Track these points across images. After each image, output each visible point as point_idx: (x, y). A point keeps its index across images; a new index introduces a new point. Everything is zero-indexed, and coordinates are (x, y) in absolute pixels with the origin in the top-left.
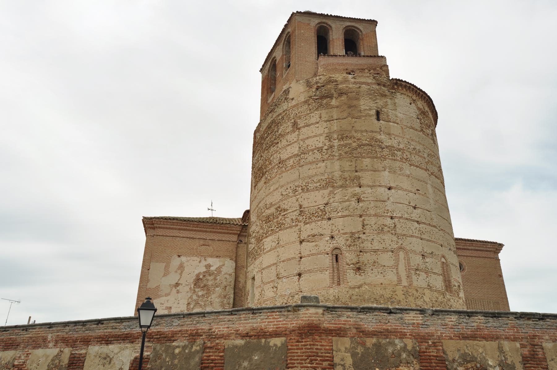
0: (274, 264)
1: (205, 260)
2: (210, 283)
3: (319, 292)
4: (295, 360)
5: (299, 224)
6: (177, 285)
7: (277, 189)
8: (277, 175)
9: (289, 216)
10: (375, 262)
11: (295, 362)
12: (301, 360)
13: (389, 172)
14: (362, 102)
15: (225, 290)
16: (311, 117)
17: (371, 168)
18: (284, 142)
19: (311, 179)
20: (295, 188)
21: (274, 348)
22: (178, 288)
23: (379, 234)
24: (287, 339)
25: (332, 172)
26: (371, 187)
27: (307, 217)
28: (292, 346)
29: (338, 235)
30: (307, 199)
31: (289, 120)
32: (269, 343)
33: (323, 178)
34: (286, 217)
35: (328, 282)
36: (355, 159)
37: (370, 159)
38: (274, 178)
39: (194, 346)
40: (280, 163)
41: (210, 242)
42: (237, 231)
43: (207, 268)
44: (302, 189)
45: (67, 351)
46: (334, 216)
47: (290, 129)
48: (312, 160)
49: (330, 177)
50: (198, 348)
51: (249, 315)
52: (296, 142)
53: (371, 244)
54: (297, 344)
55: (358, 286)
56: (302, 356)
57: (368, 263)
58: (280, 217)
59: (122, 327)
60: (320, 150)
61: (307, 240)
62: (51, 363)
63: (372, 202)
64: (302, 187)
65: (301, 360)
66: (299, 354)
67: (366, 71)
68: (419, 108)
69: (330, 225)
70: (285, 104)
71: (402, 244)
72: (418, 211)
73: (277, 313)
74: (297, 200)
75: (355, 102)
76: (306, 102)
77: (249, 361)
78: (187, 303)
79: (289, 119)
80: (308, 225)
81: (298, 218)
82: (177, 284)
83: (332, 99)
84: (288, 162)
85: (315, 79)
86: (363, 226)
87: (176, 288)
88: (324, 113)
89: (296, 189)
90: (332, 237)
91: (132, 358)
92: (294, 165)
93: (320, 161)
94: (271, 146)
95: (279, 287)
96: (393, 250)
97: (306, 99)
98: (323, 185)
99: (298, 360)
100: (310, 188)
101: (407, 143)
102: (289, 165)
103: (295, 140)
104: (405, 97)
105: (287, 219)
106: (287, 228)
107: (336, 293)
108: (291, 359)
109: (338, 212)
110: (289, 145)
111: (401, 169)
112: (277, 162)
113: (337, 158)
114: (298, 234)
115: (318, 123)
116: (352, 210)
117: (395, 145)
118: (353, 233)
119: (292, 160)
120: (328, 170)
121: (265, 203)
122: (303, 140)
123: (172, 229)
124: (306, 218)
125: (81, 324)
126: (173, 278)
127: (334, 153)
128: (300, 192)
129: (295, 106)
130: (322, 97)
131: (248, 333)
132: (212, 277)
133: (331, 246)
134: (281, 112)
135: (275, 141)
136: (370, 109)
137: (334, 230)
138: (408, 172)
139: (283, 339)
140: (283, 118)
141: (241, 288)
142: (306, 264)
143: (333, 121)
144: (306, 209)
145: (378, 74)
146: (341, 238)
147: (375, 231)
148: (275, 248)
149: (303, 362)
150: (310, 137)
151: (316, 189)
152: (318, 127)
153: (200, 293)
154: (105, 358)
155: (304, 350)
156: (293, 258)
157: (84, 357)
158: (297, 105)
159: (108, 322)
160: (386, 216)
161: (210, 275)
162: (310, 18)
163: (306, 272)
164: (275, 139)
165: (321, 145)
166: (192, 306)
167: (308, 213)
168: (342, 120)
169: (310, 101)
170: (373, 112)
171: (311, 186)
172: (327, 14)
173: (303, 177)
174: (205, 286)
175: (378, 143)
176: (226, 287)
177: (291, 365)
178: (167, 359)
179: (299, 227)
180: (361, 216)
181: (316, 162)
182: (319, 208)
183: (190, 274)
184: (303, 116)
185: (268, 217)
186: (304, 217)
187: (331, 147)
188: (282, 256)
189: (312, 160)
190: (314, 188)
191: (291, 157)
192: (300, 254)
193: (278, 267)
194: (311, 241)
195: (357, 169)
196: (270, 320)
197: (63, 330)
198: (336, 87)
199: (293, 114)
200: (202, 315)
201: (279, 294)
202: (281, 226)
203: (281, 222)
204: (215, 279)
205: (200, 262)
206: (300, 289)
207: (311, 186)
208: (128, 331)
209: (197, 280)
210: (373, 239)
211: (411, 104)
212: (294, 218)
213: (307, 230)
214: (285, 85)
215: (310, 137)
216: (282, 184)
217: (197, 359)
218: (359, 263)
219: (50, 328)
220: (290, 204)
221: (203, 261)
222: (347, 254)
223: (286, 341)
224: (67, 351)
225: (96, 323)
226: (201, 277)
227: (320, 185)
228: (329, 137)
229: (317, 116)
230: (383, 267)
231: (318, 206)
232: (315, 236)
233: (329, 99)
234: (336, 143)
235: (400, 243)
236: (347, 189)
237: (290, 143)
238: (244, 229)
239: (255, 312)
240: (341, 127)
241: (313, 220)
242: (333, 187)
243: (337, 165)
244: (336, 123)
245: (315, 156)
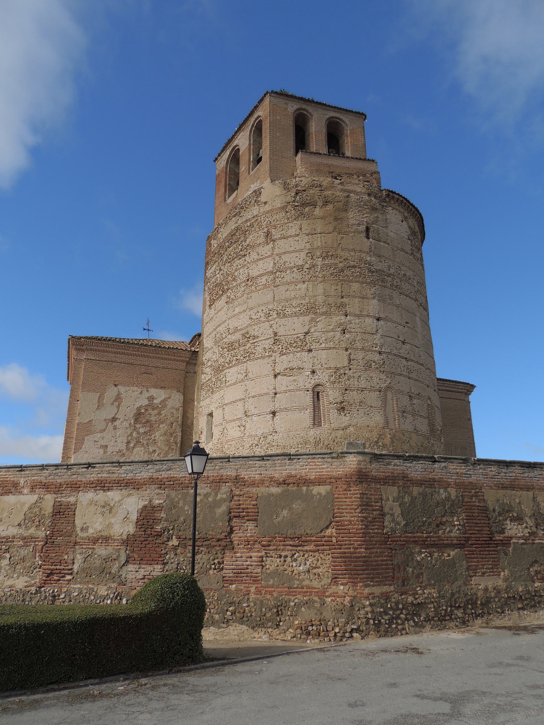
0: (240, 400)
1: (148, 391)
2: (153, 418)
3: (298, 433)
4: (343, 509)
5: (274, 354)
6: (114, 419)
7: (244, 311)
8: (245, 295)
9: (260, 344)
10: (361, 402)
11: (344, 511)
12: (351, 509)
13: (378, 300)
14: (351, 215)
15: (172, 427)
16: (290, 227)
17: (359, 295)
18: (254, 256)
19: (288, 303)
20: (268, 312)
21: (318, 496)
22: (115, 424)
23: (367, 371)
24: (333, 487)
25: (314, 296)
26: (359, 316)
27: (283, 347)
28: (339, 494)
29: (320, 369)
30: (284, 325)
31: (261, 229)
32: (311, 491)
33: (303, 302)
34: (257, 345)
35: (308, 421)
36: (341, 282)
37: (358, 283)
38: (240, 297)
39: (219, 494)
40: (248, 280)
41: (153, 370)
42: (185, 357)
43: (149, 401)
44: (277, 314)
45: (49, 499)
46: (316, 347)
47: (262, 239)
48: (290, 280)
49: (312, 301)
50: (224, 496)
51: (285, 461)
52: (269, 256)
53: (358, 381)
54: (345, 492)
55: (341, 428)
56: (352, 505)
57: (354, 403)
58: (249, 345)
59: (122, 472)
60: (300, 268)
61: (284, 374)
62: (29, 511)
63: (360, 333)
64: (277, 311)
65: (351, 509)
66: (348, 503)
67: (355, 177)
68: (410, 227)
69: (311, 358)
70: (255, 208)
71: (390, 383)
72: (406, 347)
73: (320, 460)
74: (271, 327)
75: (343, 214)
76: (283, 208)
77: (289, 510)
78: (126, 441)
79: (260, 227)
80: (284, 357)
81: (272, 347)
82: (113, 418)
83: (315, 208)
84: (259, 280)
85: (294, 181)
86: (350, 360)
87: (112, 424)
88: (305, 224)
89: (269, 313)
90: (313, 372)
91: (140, 507)
92: (267, 283)
93: (299, 282)
94: (235, 258)
95: (248, 426)
96: (380, 389)
97: (283, 205)
98: (304, 311)
99: (346, 509)
100: (287, 313)
101: (398, 268)
102: (260, 284)
103: (269, 253)
104: (397, 213)
105: (257, 348)
106: (258, 358)
107: (317, 435)
108: (338, 509)
109: (321, 344)
110: (260, 259)
111: (391, 298)
112: (245, 279)
113: (320, 279)
114: (272, 366)
115: (298, 235)
116: (337, 342)
117: (385, 270)
118: (338, 369)
119: (264, 278)
120: (311, 294)
121: (228, 327)
122: (279, 255)
123: (107, 352)
124: (282, 348)
125: (64, 467)
126: (109, 412)
127: (317, 273)
128: (275, 317)
129: (268, 212)
130: (304, 205)
131: (284, 481)
132: (156, 412)
133: (313, 382)
134: (249, 217)
135: (241, 253)
136: (359, 225)
137: (316, 364)
138: (398, 302)
139: (328, 487)
140: (252, 225)
141: (190, 425)
142: (282, 401)
143: (316, 235)
144: (282, 338)
145: (368, 182)
146: (324, 374)
147: (362, 367)
148: (242, 381)
149: (353, 511)
150: (289, 252)
151: (295, 314)
152: (298, 241)
153: (142, 430)
154: (104, 507)
155: (353, 499)
156: (266, 394)
157: (75, 504)
158: (272, 210)
159: (102, 465)
160: (375, 351)
161: (153, 410)
162: (288, 102)
163: (281, 410)
165: (300, 263)
166: (132, 445)
167: (285, 342)
168: (328, 235)
169: (288, 208)
170: (363, 228)
171: (289, 311)
172: (309, 99)
173: (279, 300)
174: (147, 421)
175: (367, 265)
176: (172, 423)
177: (338, 515)
178: (186, 508)
179: (273, 358)
180: (347, 350)
181: (296, 283)
182: (298, 337)
183: (129, 407)
184: (279, 226)
185: (231, 344)
186: (280, 346)
187: (313, 266)
188: (251, 390)
189: (290, 280)
190: (292, 313)
191: (261, 275)
192: (275, 389)
193: (246, 403)
194: (288, 375)
195: (343, 294)
196: (311, 467)
197: (39, 473)
198: (321, 193)
199: (266, 222)
200: (226, 460)
201: (247, 434)
202: (249, 356)
203: (250, 350)
204: (159, 414)
205: (141, 393)
206: (274, 429)
207: (289, 311)
208: (130, 476)
209: (138, 416)
210: (360, 376)
211: (402, 221)
212: (266, 347)
213: (283, 362)
214: (253, 184)
215: (289, 252)
216: (250, 306)
217: (223, 508)
218: (343, 402)
219: (21, 471)
220: (261, 330)
221: (145, 392)
222: (331, 392)
223: (331, 490)
224: (49, 499)
225: (85, 466)
226: (143, 411)
227: (300, 311)
228: (311, 254)
229: (297, 227)
230: (369, 408)
231: (297, 334)
232: (294, 369)
233: (311, 207)
234: (319, 262)
235: (388, 382)
236: (331, 317)
237: (261, 257)
238: (194, 355)
239: (292, 457)
240: (326, 243)
241: (291, 351)
242: (315, 313)
243: (320, 288)
244: (319, 238)
245: (294, 275)
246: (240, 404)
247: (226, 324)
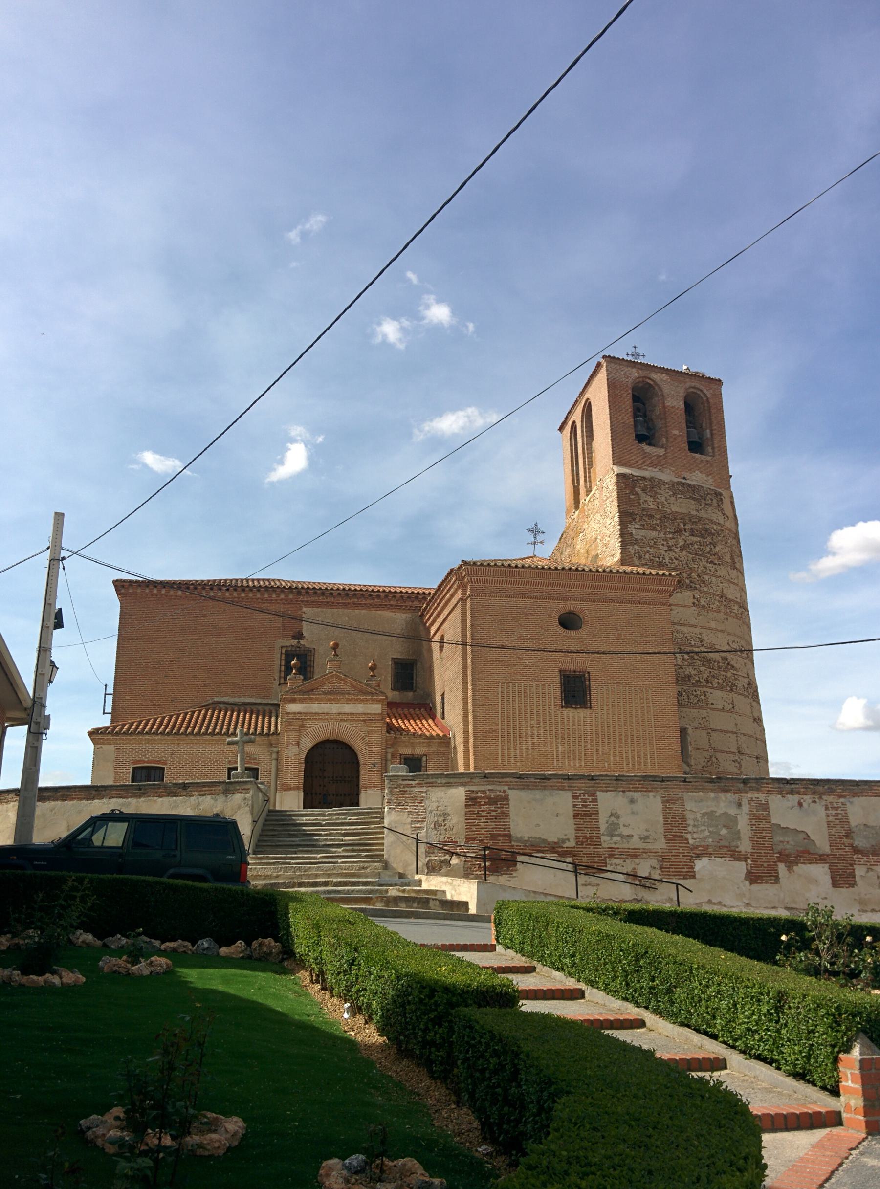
0: (733, 733)
7: (721, 631)
112: (718, 593)
164: (709, 553)
214: (701, 472)
246: (733, 736)
247: (698, 630)
